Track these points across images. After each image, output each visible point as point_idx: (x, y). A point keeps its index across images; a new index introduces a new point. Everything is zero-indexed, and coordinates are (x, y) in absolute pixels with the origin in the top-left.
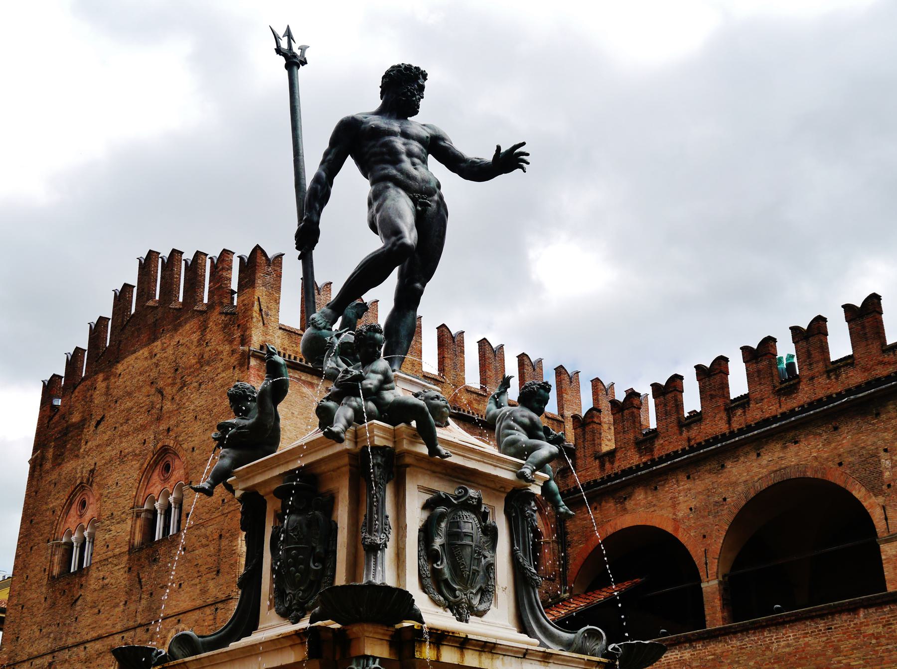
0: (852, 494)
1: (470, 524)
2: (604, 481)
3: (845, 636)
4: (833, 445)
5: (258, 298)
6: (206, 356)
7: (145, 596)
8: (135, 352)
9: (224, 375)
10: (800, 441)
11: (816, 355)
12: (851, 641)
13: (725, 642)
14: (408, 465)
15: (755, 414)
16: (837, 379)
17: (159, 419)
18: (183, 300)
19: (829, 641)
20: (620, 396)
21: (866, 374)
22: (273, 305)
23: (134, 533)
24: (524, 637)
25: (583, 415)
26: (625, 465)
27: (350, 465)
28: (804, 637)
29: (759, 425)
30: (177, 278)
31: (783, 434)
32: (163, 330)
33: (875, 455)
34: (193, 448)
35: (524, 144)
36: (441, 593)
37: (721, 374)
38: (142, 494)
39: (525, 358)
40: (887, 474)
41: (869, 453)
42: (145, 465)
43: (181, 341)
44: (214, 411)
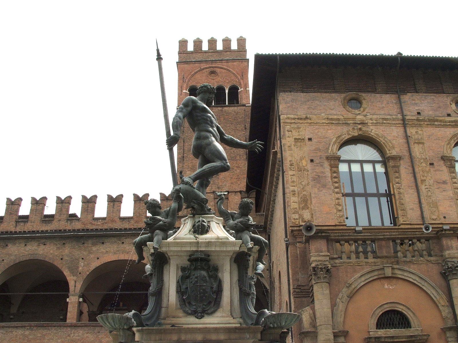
0: (63, 273)
3: (105, 336)
4: (61, 251)
10: (47, 245)
11: (64, 210)
12: (107, 339)
13: (49, 329)
15: (28, 227)
16: (70, 224)
19: (97, 337)
21: (83, 226)
28: (86, 334)
29: (29, 232)
31: (40, 239)
33: (78, 260)
37: (18, 205)
40: (81, 268)
41: (75, 258)
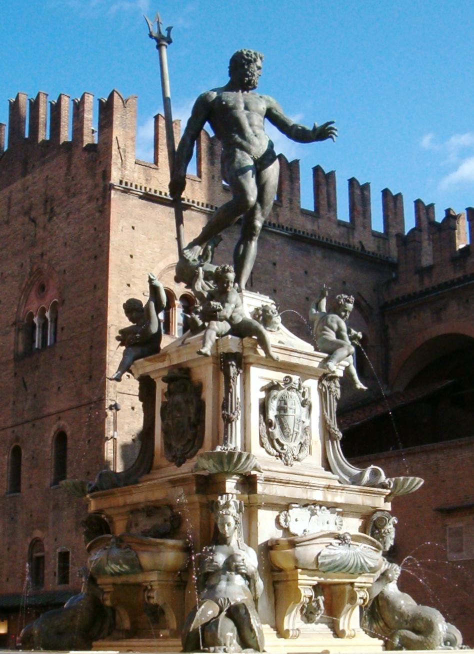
1: (294, 399)
2: (422, 293)
5: (117, 138)
6: (73, 191)
7: (30, 397)
8: (10, 183)
9: (89, 207)
14: (251, 364)
17: (33, 245)
18: (50, 138)
20: (439, 217)
22: (129, 143)
23: (18, 344)
24: (329, 474)
25: (406, 234)
26: (442, 280)
27: (214, 363)
30: (43, 118)
32: (33, 166)
34: (65, 271)
35: (332, 123)
36: (274, 447)
38: (22, 311)
39: (354, 182)
42: (24, 286)
43: (49, 177)
44: (82, 238)
